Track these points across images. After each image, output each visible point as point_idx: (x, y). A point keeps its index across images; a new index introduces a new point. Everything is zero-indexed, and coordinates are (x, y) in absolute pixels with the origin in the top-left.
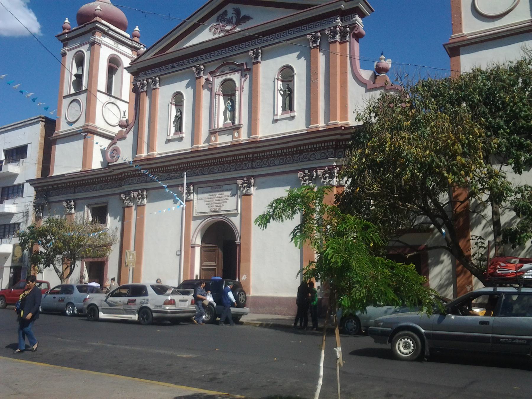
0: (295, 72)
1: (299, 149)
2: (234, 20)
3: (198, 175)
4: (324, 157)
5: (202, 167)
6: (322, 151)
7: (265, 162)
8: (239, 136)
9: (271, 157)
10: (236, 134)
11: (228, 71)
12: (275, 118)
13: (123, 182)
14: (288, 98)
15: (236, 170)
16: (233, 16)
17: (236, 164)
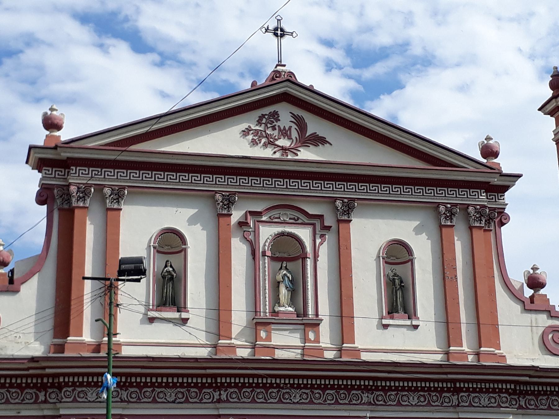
0: (416, 253)
1: (458, 385)
2: (295, 134)
3: (254, 401)
4: (495, 405)
5: (264, 386)
6: (492, 395)
7: (392, 397)
8: (317, 340)
9: (404, 390)
10: (311, 336)
11: (287, 220)
12: (385, 322)
13: (43, 393)
14: (399, 293)
15: (337, 403)
16: (292, 127)
17: (338, 393)
